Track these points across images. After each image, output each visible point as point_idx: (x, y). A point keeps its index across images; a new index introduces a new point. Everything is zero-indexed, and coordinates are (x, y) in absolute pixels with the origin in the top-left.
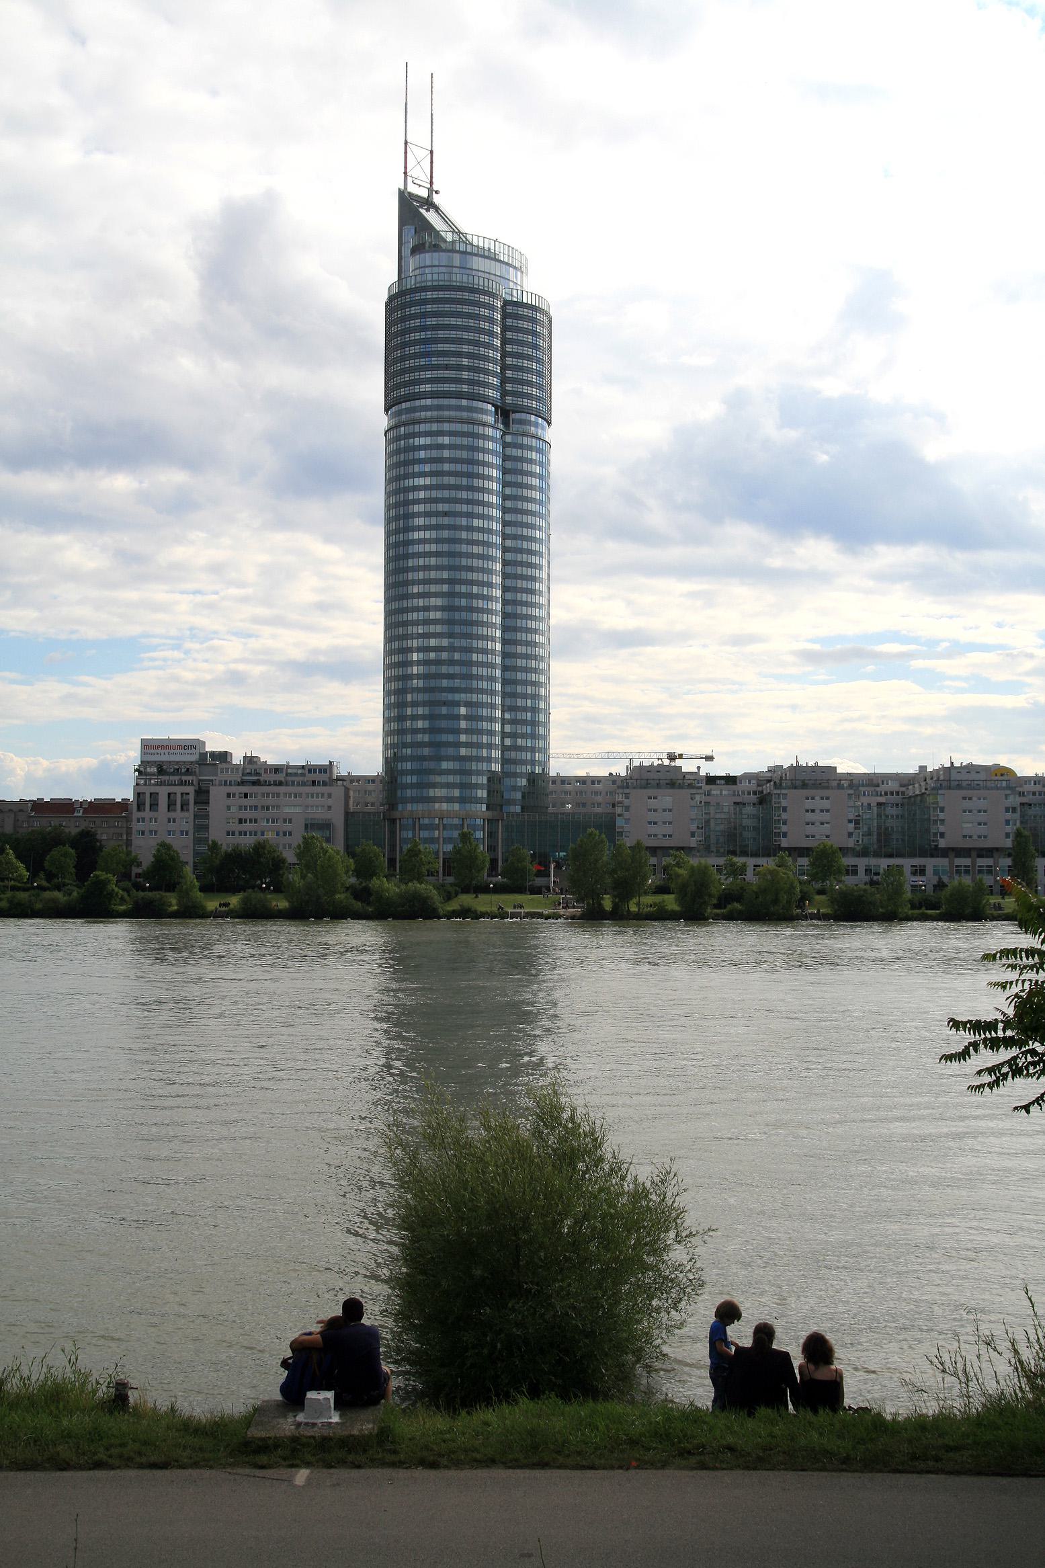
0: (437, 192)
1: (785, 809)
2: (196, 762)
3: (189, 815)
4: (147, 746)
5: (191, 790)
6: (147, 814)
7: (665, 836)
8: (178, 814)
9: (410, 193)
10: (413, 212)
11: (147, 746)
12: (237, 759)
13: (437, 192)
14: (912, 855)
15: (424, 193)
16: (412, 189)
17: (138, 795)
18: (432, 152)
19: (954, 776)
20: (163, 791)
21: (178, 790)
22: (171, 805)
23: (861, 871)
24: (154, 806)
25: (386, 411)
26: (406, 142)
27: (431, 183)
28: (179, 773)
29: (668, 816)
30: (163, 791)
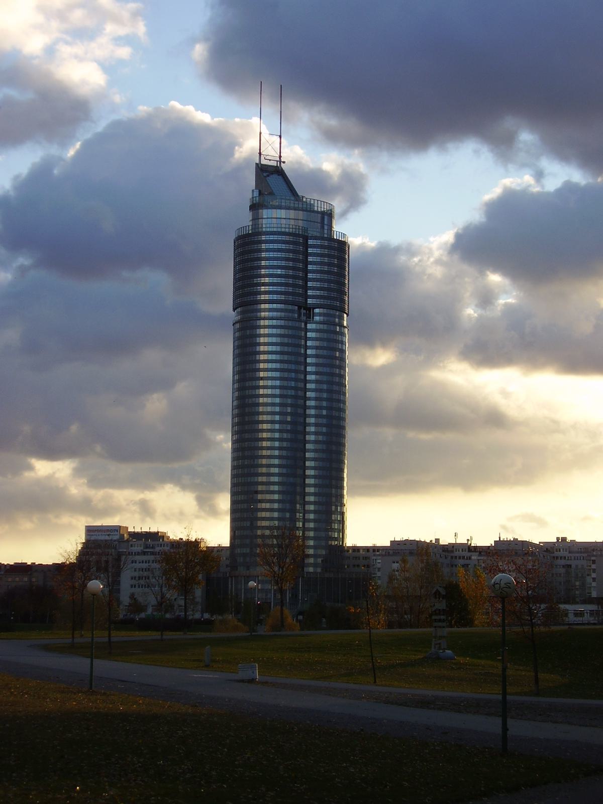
0: (284, 162)
11: (90, 530)
15: (274, 164)
16: (264, 162)
25: (234, 310)
27: (280, 157)
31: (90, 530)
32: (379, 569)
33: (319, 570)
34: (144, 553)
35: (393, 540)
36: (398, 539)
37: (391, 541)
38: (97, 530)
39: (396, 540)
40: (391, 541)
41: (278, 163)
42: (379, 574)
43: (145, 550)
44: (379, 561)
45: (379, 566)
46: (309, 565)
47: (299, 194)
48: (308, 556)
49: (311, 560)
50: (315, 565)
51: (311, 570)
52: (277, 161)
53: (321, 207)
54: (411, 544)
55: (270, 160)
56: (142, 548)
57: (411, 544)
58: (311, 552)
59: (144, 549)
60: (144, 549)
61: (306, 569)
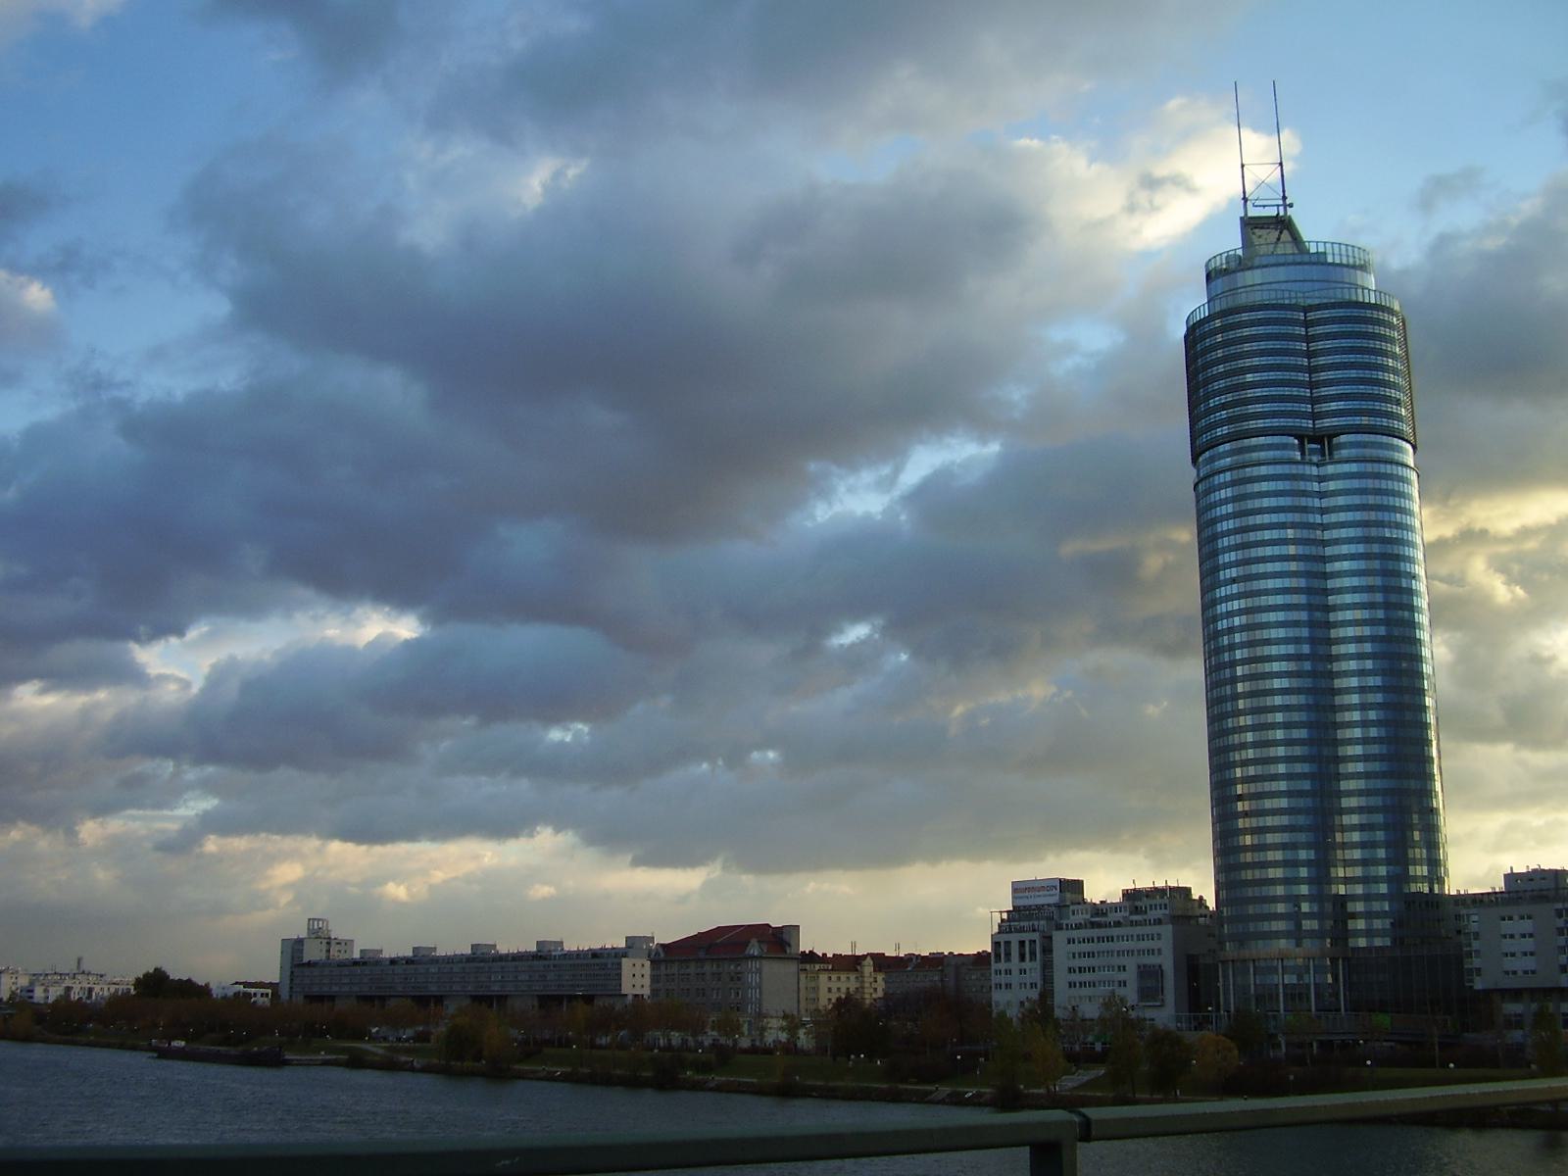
0: (1291, 206)
2: (1055, 905)
3: (1037, 965)
6: (1002, 966)
7: (1526, 972)
8: (1027, 964)
9: (1251, 218)
11: (1018, 889)
13: (1291, 206)
15: (1273, 212)
16: (1253, 212)
17: (996, 944)
18: (1281, 164)
20: (1014, 938)
21: (1027, 937)
22: (1022, 958)
26: (1243, 166)
27: (1284, 198)
29: (1528, 944)
31: (1018, 889)
32: (1477, 936)
33: (1388, 942)
34: (1093, 925)
35: (1509, 872)
36: (1520, 869)
37: (1505, 875)
38: (1040, 889)
39: (1515, 871)
40: (1505, 875)
41: (1281, 208)
42: (1476, 945)
43: (1093, 919)
44: (1475, 918)
45: (1474, 927)
46: (1357, 933)
48: (1354, 916)
49: (1361, 924)
50: (1369, 933)
51: (1362, 942)
52: (1278, 206)
53: (1348, 256)
54: (1544, 879)
55: (1264, 206)
56: (1088, 917)
57: (1544, 879)
58: (1360, 907)
59: (1092, 917)
60: (1092, 917)
61: (1352, 943)
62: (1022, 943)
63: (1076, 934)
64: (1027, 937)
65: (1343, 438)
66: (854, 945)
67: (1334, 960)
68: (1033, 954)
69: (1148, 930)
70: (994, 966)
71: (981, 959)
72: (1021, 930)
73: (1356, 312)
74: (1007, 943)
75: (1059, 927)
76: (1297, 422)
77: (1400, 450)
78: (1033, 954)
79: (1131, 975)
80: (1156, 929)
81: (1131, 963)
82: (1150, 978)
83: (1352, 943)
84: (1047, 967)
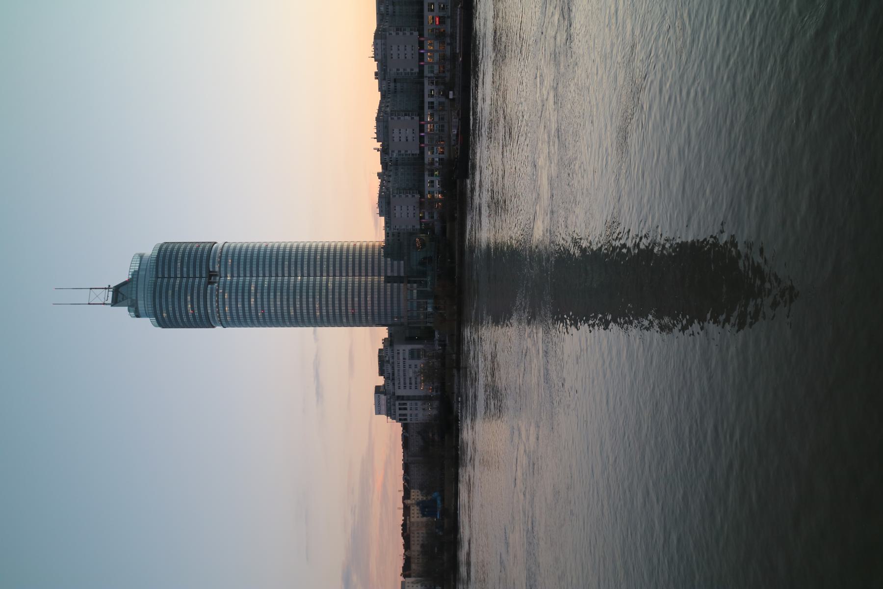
1: (398, 70)
3: (408, 403)
4: (378, 412)
5: (397, 403)
6: (408, 418)
8: (408, 406)
10: (120, 295)
11: (378, 412)
12: (381, 381)
14: (422, 84)
15: (111, 294)
16: (110, 301)
17: (400, 420)
19: (379, 57)
20: (398, 412)
21: (397, 407)
22: (405, 409)
23: (431, 100)
24: (405, 415)
28: (389, 400)
30: (398, 412)
34: (393, 379)
47: (126, 279)
61: (402, 274)
62: (400, 409)
63: (396, 387)
64: (397, 407)
65: (211, 267)
66: (399, 508)
67: (409, 282)
68: (405, 404)
69: (396, 355)
70: (409, 421)
71: (405, 427)
72: (395, 410)
73: (160, 263)
74: (400, 415)
75: (394, 394)
76: (202, 286)
77: (217, 248)
78: (405, 404)
79: (414, 362)
80: (396, 352)
81: (408, 362)
82: (413, 355)
83: (402, 274)
84: (409, 398)
